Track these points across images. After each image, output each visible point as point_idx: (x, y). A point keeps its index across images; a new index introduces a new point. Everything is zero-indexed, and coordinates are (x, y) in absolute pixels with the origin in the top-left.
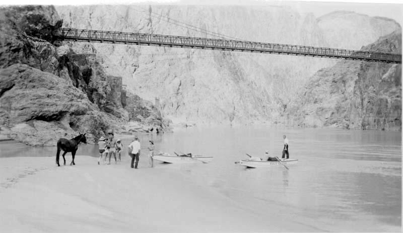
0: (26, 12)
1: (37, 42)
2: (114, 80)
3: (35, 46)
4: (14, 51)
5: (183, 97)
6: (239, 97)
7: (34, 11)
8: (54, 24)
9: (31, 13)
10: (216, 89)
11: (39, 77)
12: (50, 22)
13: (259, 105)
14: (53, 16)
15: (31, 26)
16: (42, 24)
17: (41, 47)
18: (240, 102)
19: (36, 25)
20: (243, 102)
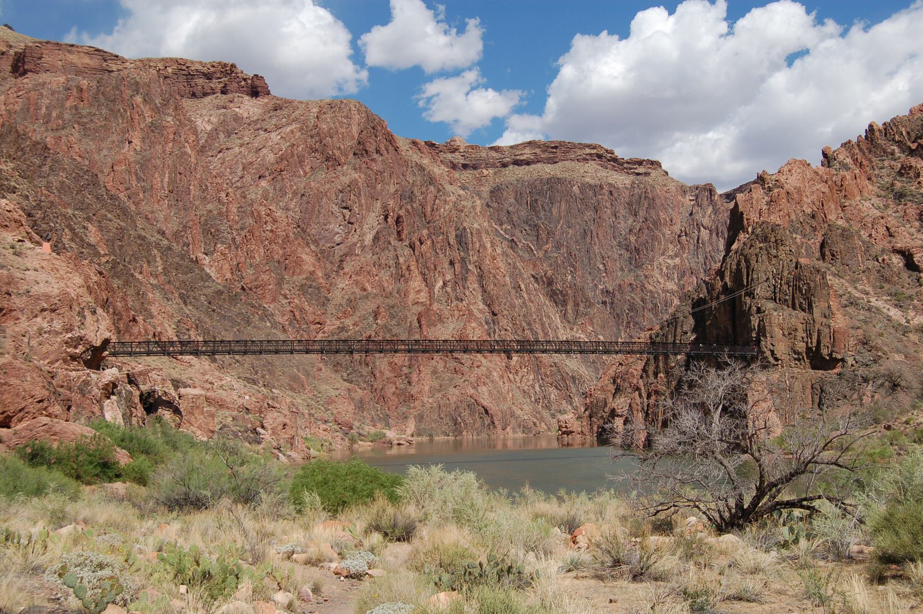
0: (64, 334)
1: (74, 372)
2: (193, 398)
3: (72, 378)
4: (39, 402)
5: (410, 383)
6: (532, 377)
7: (73, 332)
8: (98, 344)
9: (70, 335)
10: (475, 365)
11: (61, 430)
12: (94, 341)
13: (574, 390)
14: (98, 334)
15: (69, 350)
16: (84, 346)
17: (79, 377)
18: (534, 387)
19: (76, 347)
20: (540, 386)
